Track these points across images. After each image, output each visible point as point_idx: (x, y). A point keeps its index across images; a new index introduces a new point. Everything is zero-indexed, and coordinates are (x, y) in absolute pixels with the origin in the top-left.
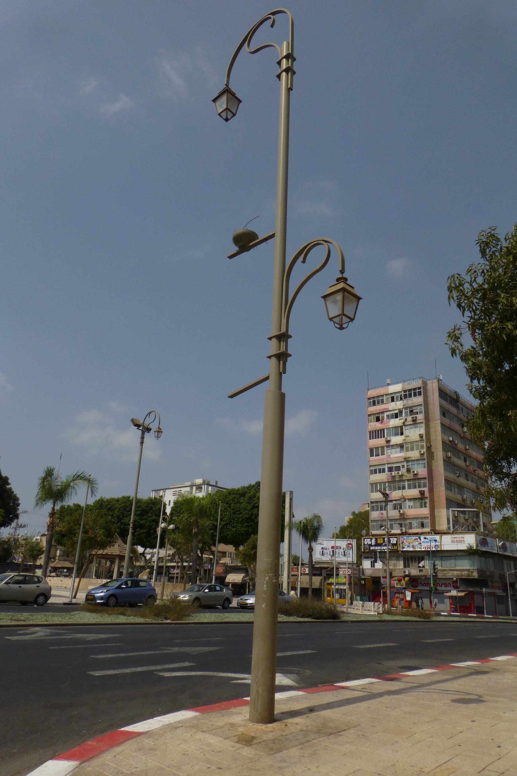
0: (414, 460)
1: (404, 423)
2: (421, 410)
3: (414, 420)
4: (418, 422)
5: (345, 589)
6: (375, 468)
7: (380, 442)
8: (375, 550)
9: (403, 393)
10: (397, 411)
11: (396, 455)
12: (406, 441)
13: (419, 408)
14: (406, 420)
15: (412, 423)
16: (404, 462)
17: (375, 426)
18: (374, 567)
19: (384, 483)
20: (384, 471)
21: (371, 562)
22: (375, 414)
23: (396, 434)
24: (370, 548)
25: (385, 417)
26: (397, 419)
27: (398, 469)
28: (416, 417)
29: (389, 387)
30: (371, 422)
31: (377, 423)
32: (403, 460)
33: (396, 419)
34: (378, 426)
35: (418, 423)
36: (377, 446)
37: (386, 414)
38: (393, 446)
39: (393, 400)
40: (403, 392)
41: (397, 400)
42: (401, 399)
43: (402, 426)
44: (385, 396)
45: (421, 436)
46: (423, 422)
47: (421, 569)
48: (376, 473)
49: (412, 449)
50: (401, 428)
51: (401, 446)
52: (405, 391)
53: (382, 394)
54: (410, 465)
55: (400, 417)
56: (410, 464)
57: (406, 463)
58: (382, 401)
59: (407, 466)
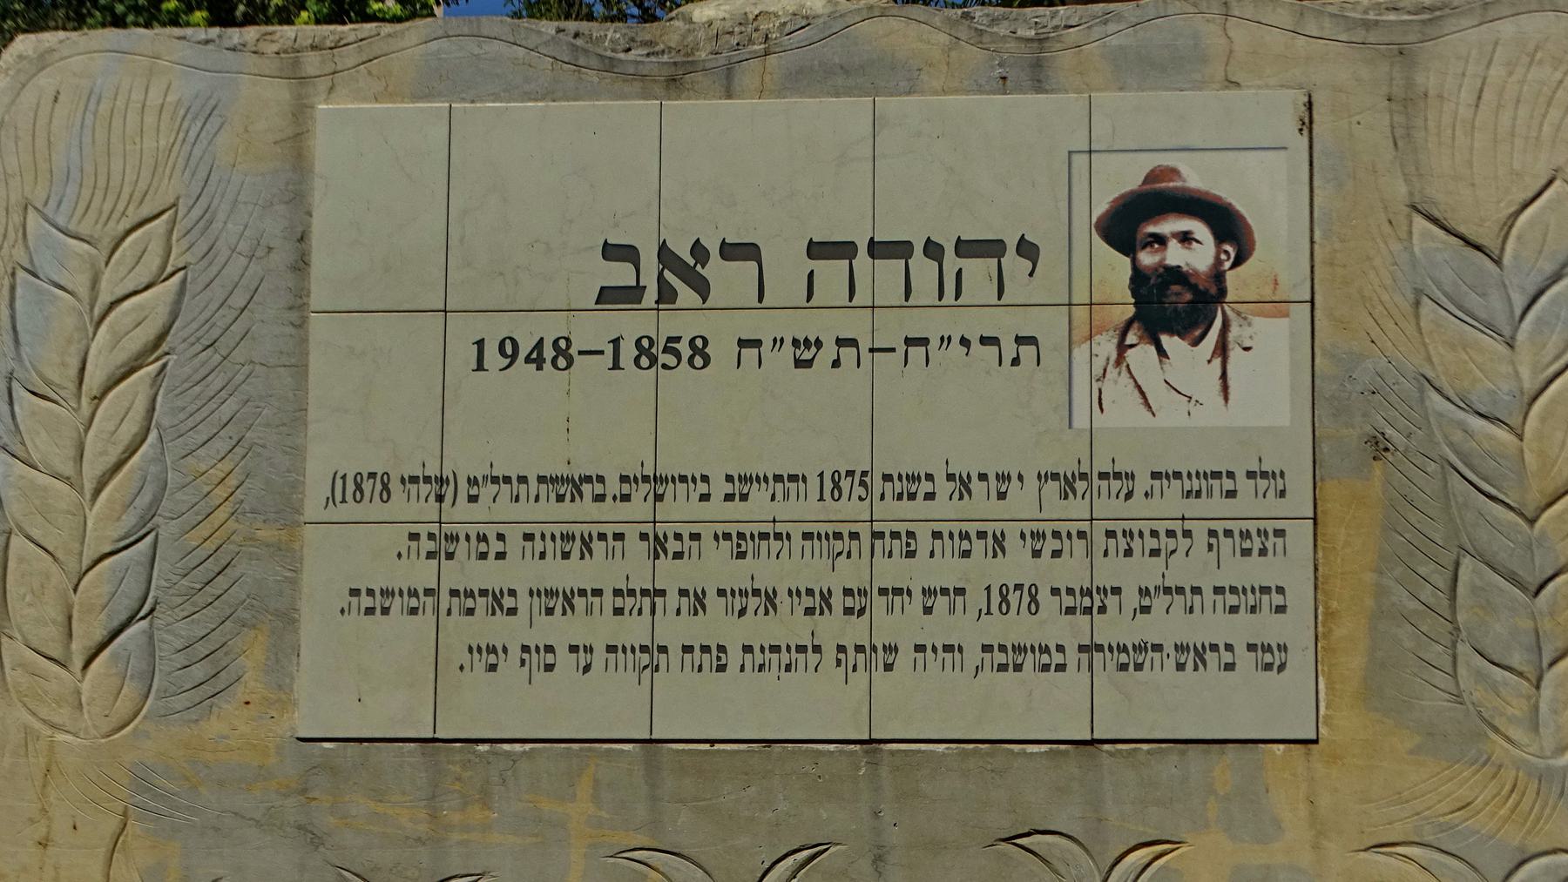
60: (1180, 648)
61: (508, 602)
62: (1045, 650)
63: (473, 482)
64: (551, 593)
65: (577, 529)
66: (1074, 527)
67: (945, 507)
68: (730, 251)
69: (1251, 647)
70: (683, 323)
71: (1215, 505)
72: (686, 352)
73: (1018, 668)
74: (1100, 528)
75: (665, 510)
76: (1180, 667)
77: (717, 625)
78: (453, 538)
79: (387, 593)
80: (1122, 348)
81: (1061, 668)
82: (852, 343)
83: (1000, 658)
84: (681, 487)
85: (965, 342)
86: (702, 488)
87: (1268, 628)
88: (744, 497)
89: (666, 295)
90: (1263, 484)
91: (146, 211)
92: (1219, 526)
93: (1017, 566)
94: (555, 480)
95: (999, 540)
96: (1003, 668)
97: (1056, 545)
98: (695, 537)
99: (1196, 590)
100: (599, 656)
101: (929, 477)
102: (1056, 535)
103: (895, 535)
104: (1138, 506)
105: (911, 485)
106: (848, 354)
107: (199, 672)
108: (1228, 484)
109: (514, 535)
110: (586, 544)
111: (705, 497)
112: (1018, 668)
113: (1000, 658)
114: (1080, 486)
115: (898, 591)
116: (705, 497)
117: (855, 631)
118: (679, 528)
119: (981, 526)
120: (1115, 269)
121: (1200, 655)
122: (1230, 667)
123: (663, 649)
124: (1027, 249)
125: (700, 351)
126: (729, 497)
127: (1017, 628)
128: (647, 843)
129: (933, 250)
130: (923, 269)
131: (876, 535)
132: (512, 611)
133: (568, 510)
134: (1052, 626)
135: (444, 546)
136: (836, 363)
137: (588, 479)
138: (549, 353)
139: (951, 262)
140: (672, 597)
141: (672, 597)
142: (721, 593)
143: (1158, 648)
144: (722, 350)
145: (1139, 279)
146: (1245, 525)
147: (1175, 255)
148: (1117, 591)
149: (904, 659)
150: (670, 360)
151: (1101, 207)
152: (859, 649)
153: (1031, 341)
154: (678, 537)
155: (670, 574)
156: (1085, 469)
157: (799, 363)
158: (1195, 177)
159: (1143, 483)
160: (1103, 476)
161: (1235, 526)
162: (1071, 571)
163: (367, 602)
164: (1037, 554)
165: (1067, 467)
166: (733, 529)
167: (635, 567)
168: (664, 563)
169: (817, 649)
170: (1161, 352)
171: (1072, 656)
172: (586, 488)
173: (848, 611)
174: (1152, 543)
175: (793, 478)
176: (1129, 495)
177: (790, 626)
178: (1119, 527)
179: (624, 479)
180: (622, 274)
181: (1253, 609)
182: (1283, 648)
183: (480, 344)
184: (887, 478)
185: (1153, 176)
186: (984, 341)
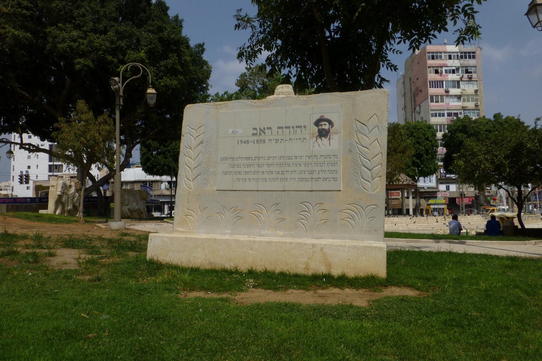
0: (470, 110)
1: (461, 78)
2: (475, 71)
3: (470, 78)
4: (473, 79)
5: (444, 208)
6: (436, 112)
7: (440, 91)
8: (450, 177)
9: (459, 55)
10: (454, 68)
11: (454, 104)
12: (464, 94)
13: (473, 68)
14: (463, 76)
15: (468, 80)
16: (461, 110)
17: (432, 76)
18: (449, 190)
19: (444, 125)
20: (443, 115)
21: (447, 186)
22: (435, 67)
23: (454, 87)
24: (446, 176)
25: (444, 71)
26: (455, 74)
27: (456, 114)
28: (472, 76)
29: (447, 46)
30: (430, 73)
31: (436, 75)
32: (461, 108)
33: (453, 74)
34: (437, 77)
35: (473, 81)
36: (437, 94)
37: (444, 69)
38: (451, 96)
39: (450, 58)
40: (459, 53)
41: (454, 59)
42: (458, 59)
43: (459, 81)
44: (443, 53)
45: (476, 91)
46: (477, 81)
47: (488, 190)
48: (436, 116)
49: (468, 101)
50: (458, 82)
51: (459, 97)
52: (462, 53)
53: (441, 51)
54: (466, 113)
55: (457, 73)
56: (467, 112)
57: (464, 111)
58: (441, 57)
59: (464, 113)
60: (323, 178)
61: (241, 173)
62: (306, 179)
63: (237, 158)
64: (246, 172)
65: (249, 164)
66: (310, 163)
67: (294, 160)
68: (268, 128)
69: (333, 178)
70: (262, 137)
71: (328, 159)
72: (262, 141)
73: (303, 181)
74: (313, 162)
75: (260, 161)
76: (323, 181)
77: (266, 176)
78: (235, 165)
79: (227, 172)
80: (317, 139)
81: (308, 181)
82: (283, 139)
83: (300, 180)
84: (262, 158)
85: (297, 139)
86: (264, 158)
87: (335, 176)
88: (269, 159)
89: (260, 134)
90: (334, 156)
91: (200, 126)
92: (329, 162)
93: (303, 168)
94: (247, 158)
95: (301, 165)
96: (301, 181)
97: (308, 165)
98: (263, 165)
99: (325, 171)
100: (251, 180)
101: (292, 157)
102: (308, 164)
103: (288, 164)
104: (318, 160)
105: (290, 158)
106: (282, 141)
107: (205, 182)
108: (330, 157)
109: (242, 165)
110: (250, 166)
111: (264, 160)
112: (303, 181)
113: (300, 180)
114: (311, 157)
115: (288, 171)
116: (264, 160)
117: (282, 176)
118: (261, 164)
119: (298, 163)
120: (316, 129)
121: (326, 179)
122: (330, 181)
123: (259, 179)
124: (305, 127)
125: (264, 141)
126: (267, 160)
127: (303, 176)
128: (257, 203)
129: (293, 127)
130: (292, 130)
131: (285, 164)
132: (241, 174)
133: (248, 161)
134: (308, 176)
135: (233, 166)
136: (281, 142)
137: (250, 158)
138: (246, 142)
139: (295, 129)
140: (260, 172)
141: (260, 172)
142: (266, 172)
143: (320, 178)
144: (267, 141)
145: (319, 131)
146: (332, 162)
147: (324, 127)
148: (315, 171)
149: (289, 180)
150: (261, 142)
151: (314, 121)
152: (283, 179)
153: (305, 139)
154: (261, 165)
155: (260, 169)
156: (312, 155)
157: (276, 142)
158: (326, 116)
159: (319, 157)
160: (314, 156)
161: (331, 162)
162: (310, 168)
163: (224, 173)
164: (305, 166)
165: (309, 155)
166: (268, 164)
167: (256, 168)
168: (260, 168)
169: (278, 179)
170: (322, 140)
171: (309, 179)
172: (250, 159)
173: (282, 174)
174: (320, 165)
175: (275, 157)
176: (317, 158)
177: (275, 176)
178: (316, 162)
179: (255, 157)
180: (255, 132)
181: (333, 173)
182: (337, 178)
183: (238, 141)
184: (287, 157)
185: (321, 117)
186: (299, 139)
